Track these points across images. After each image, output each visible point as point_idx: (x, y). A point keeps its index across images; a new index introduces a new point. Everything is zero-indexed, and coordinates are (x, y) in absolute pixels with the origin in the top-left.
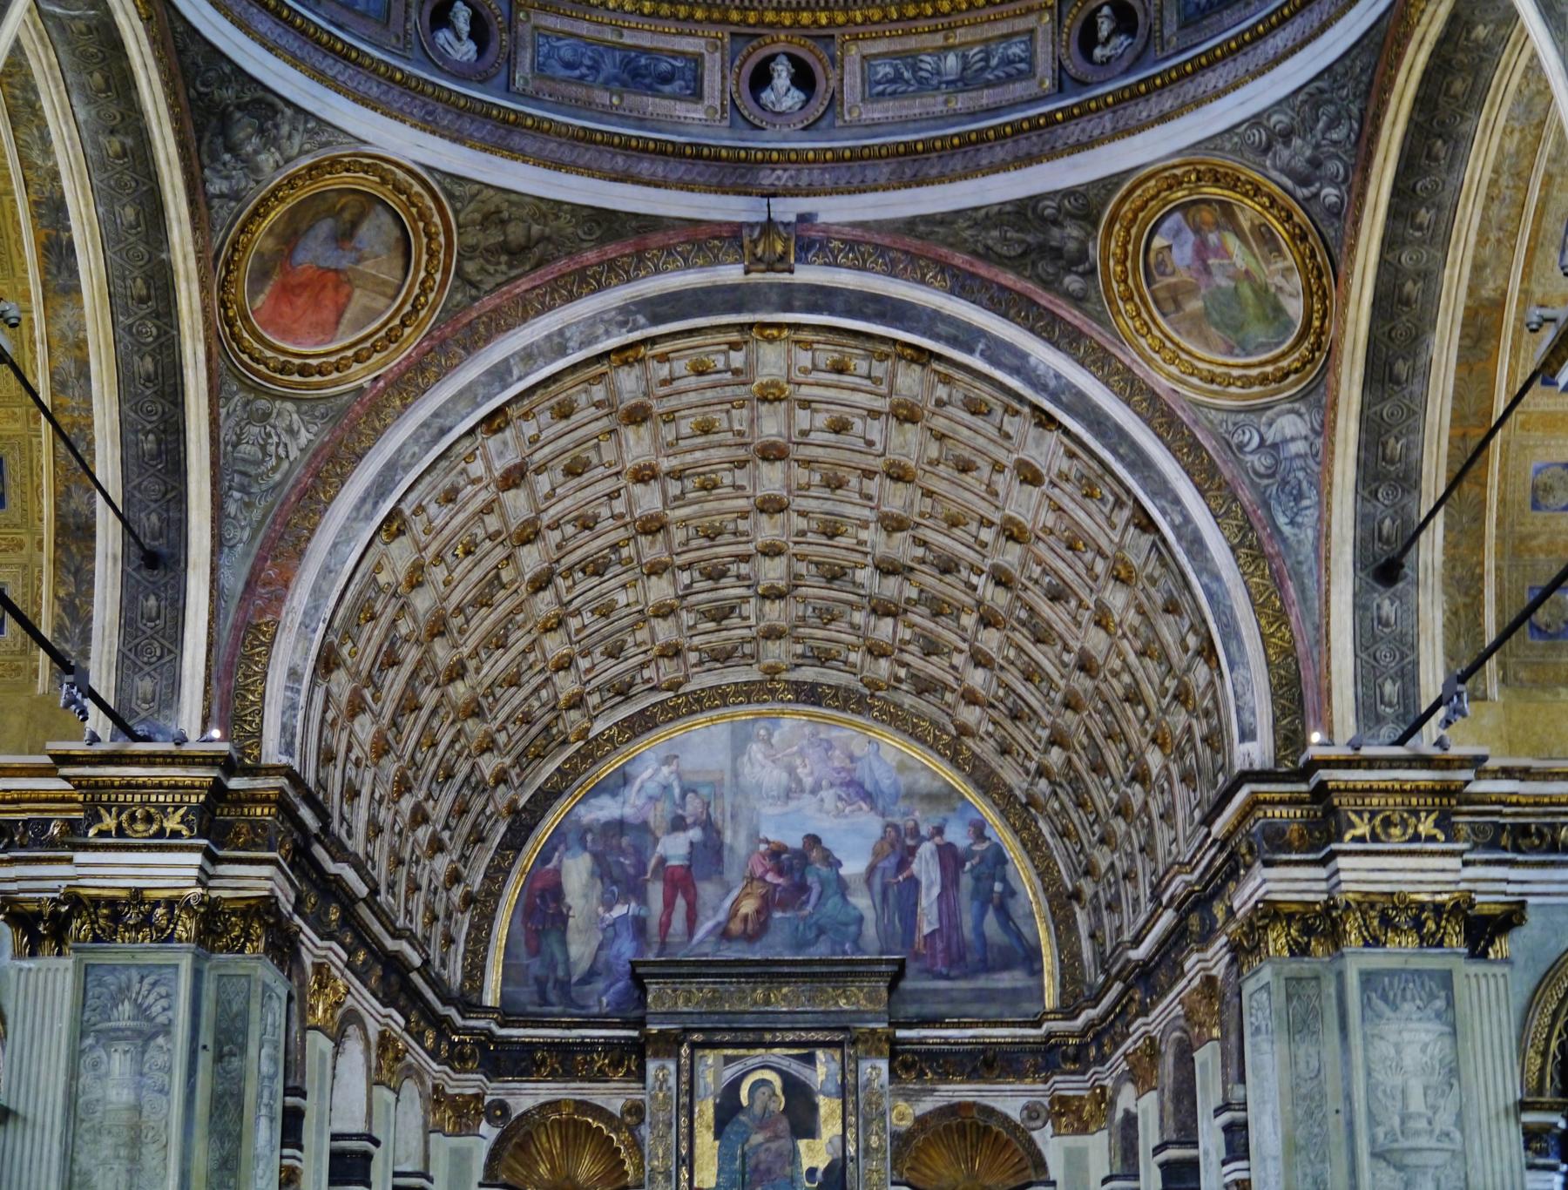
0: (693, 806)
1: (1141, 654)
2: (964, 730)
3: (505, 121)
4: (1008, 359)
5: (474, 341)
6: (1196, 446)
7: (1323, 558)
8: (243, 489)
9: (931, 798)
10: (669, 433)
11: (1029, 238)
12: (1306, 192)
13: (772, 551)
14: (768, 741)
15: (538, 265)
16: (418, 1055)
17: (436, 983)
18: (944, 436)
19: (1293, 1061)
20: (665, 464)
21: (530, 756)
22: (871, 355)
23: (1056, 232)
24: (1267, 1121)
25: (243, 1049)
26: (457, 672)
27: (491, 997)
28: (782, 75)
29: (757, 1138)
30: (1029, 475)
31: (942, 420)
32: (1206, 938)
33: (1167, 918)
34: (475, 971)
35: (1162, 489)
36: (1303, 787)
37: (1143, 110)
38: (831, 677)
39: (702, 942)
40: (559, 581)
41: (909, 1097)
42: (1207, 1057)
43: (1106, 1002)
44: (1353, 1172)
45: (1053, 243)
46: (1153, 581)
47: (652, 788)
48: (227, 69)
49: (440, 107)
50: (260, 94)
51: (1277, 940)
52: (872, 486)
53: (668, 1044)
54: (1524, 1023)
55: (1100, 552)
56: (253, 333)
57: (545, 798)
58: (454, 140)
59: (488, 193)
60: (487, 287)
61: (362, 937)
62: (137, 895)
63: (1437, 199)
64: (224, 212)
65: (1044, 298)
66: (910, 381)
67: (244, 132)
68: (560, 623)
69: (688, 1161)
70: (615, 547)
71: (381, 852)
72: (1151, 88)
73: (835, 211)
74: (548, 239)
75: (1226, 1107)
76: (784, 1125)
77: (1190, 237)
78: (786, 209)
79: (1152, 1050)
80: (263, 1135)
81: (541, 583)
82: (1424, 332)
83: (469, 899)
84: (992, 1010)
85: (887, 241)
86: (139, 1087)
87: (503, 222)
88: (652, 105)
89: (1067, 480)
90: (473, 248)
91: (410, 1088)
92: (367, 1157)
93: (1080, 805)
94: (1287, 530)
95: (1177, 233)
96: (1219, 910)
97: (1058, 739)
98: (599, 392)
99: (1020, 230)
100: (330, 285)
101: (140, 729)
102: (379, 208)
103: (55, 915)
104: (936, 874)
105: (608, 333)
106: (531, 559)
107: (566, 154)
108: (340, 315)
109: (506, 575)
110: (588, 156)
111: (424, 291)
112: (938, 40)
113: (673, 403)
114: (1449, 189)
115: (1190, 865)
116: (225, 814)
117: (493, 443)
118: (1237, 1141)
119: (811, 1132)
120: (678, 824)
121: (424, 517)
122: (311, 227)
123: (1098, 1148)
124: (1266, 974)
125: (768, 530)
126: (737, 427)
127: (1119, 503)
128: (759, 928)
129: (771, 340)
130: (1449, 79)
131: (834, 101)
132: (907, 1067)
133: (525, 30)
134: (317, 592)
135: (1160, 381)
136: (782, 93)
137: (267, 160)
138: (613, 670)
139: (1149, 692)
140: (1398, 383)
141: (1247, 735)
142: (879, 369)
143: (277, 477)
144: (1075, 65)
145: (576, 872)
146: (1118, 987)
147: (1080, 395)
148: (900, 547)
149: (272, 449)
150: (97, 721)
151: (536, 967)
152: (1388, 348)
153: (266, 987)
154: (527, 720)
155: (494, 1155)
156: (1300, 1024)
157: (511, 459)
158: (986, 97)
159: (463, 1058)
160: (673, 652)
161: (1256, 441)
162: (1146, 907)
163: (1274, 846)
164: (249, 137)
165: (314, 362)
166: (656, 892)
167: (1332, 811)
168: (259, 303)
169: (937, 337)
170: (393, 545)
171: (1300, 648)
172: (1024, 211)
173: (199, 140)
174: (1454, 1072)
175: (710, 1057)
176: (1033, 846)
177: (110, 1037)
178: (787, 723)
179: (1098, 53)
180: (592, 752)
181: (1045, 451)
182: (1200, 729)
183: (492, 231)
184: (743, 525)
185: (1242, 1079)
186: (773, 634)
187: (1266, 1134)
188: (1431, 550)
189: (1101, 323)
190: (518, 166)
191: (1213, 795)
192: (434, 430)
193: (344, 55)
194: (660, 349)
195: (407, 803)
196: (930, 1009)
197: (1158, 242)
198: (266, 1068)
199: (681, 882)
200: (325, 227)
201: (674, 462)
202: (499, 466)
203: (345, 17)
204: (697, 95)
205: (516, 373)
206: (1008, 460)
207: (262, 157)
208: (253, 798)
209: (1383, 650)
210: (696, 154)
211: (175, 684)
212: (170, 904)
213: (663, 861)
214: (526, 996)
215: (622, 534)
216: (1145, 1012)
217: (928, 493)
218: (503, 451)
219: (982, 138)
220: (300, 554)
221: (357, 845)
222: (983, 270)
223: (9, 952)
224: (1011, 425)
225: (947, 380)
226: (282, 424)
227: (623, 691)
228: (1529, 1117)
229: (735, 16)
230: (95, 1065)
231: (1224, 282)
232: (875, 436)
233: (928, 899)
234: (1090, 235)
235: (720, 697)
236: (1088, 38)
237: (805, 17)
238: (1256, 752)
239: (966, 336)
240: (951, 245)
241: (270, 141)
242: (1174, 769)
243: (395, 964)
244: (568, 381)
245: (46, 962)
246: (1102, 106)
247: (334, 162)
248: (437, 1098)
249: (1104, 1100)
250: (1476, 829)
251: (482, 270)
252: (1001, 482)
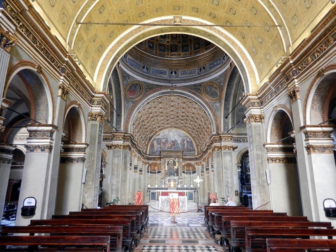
0: (165, 137)
1: (204, 124)
2: (189, 130)
4: (193, 98)
5: (146, 96)
7: (221, 116)
8: (126, 109)
9: (186, 136)
10: (163, 104)
11: (195, 87)
12: (219, 84)
13: (172, 115)
14: (172, 131)
15: (152, 89)
16: (141, 158)
17: (143, 152)
19: (217, 160)
20: (163, 107)
21: (151, 133)
22: (181, 98)
24: (215, 165)
25: (127, 158)
26: (145, 125)
27: (148, 154)
28: (173, 72)
29: (171, 166)
30: (195, 109)
32: (210, 149)
33: (207, 147)
34: (146, 151)
35: (207, 110)
36: (219, 136)
37: (206, 76)
38: (177, 126)
39: (166, 149)
41: (184, 162)
42: (210, 159)
43: (201, 155)
44: (222, 169)
46: (205, 117)
47: (162, 135)
51: (216, 149)
52: (181, 109)
53: (163, 158)
54: (237, 156)
55: (201, 115)
56: (128, 96)
57: (152, 136)
60: (148, 91)
61: (137, 148)
62: (118, 145)
65: (196, 93)
66: (184, 100)
68: (154, 121)
69: (165, 168)
70: (159, 114)
71: (138, 141)
72: (206, 75)
73: (178, 85)
75: (211, 164)
76: (173, 165)
77: (209, 88)
78: (174, 85)
79: (205, 159)
80: (129, 165)
81: (152, 117)
83: (146, 145)
84: (191, 155)
85: (182, 88)
86: (118, 161)
88: (162, 75)
91: (141, 161)
92: (137, 167)
93: (199, 137)
94: (218, 113)
95: (208, 87)
96: (211, 146)
97: (197, 131)
98: (157, 101)
101: (118, 130)
103: (110, 146)
104: (186, 143)
106: (151, 115)
107: (155, 80)
112: (187, 70)
113: (164, 102)
115: (209, 143)
116: (125, 137)
117: (148, 105)
118: (212, 167)
119: (175, 165)
120: (164, 139)
123: (200, 167)
124: (215, 152)
125: (172, 113)
127: (203, 111)
128: (171, 148)
131: (178, 75)
132: (184, 160)
133: (151, 69)
134: (133, 118)
135: (207, 100)
136: (174, 74)
137: (129, 81)
138: (158, 125)
139: (205, 127)
141: (214, 131)
144: (200, 72)
145: (155, 143)
146: (202, 153)
148: (184, 114)
150: (115, 130)
151: (151, 151)
153: (129, 153)
154: (151, 129)
155: (148, 167)
156: (218, 157)
157: (149, 107)
158: (192, 75)
159: (145, 159)
160: (163, 123)
162: (205, 146)
163: (216, 141)
166: (162, 144)
167: (221, 138)
171: (218, 124)
172: (195, 85)
174: (231, 161)
175: (167, 159)
176: (195, 141)
177: (116, 157)
178: (173, 130)
179: (201, 71)
180: (156, 132)
181: (196, 106)
182: (209, 131)
184: (170, 112)
185: (213, 161)
186: (172, 122)
187: (215, 166)
188: (230, 116)
189: (201, 95)
191: (211, 137)
193: (135, 71)
194: (163, 97)
195: (140, 136)
196: (186, 155)
197: (206, 88)
198: (129, 159)
199: (164, 144)
203: (135, 68)
204: (166, 74)
206: (193, 107)
208: (127, 136)
209: (226, 124)
210: (166, 80)
211: (121, 126)
212: (121, 145)
213: (163, 142)
214: (151, 153)
215: (159, 113)
216: (204, 155)
217: (186, 110)
218: (148, 106)
219: (191, 78)
220: (131, 115)
221: (136, 140)
222: (191, 90)
223: (106, 150)
224: (193, 104)
225: (188, 100)
227: (159, 127)
228: (238, 165)
230: (114, 159)
231: (212, 91)
233: (186, 145)
234: (201, 87)
235: (168, 127)
236: (201, 70)
237: (176, 67)
238: (214, 133)
239: (189, 96)
242: (207, 134)
243: (139, 151)
244: (154, 100)
245: (110, 150)
246: (202, 76)
247: (135, 81)
248: (143, 162)
249: (201, 163)
250: (234, 140)
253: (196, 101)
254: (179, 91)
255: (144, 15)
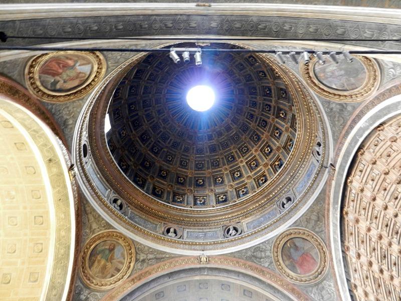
3: (295, 207)
6: (390, 90)
11: (337, 115)
15: (324, 217)
18: (381, 155)
20: (368, 223)
23: (334, 109)
31: (377, 154)
40: (383, 267)
45: (338, 110)
48: (244, 251)
49: (285, 217)
50: (254, 248)
52: (388, 181)
56: (303, 277)
58: (290, 218)
59: (301, 219)
63: (281, 24)
64: (273, 267)
65: (353, 117)
66: (367, 156)
67: (259, 254)
70: (381, 248)
74: (318, 212)
77: (329, 79)
81: (381, 271)
82: (329, 23)
85: (337, 146)
87: (310, 219)
89: (397, 129)
90: (313, 227)
99: (335, 117)
100: (306, 257)
102: (294, 239)
105: (337, 214)
106: (375, 267)
108: (314, 259)
109: (376, 276)
110: (308, 195)
111: (317, 241)
114: (279, 20)
121: (357, 280)
122: (290, 253)
126: (366, 201)
129: (351, 182)
130: (235, 29)
135: (374, 93)
137: (268, 253)
140: (345, 32)
142: (364, 162)
143: (336, 296)
147: (371, 117)
149: (330, 292)
152: (331, 36)
161: (392, 70)
164: (261, 254)
165: (319, 270)
168: (299, 271)
169: (355, 146)
170: (358, 291)
173: (255, 263)
183: (311, 222)
184: (388, 217)
189: (360, 103)
190: (302, 209)
192: (338, 261)
200: (292, 250)
201: (369, 220)
202: (354, 256)
205: (337, 237)
206: (389, 143)
207: (267, 254)
222: (346, 128)
226: (327, 286)
229: (310, 151)
232: (377, 172)
239: (355, 140)
240: (341, 133)
241: (265, 251)
251: (319, 228)
252: (394, 148)
253: (367, 128)
254: (340, 160)
255: (42, 217)
